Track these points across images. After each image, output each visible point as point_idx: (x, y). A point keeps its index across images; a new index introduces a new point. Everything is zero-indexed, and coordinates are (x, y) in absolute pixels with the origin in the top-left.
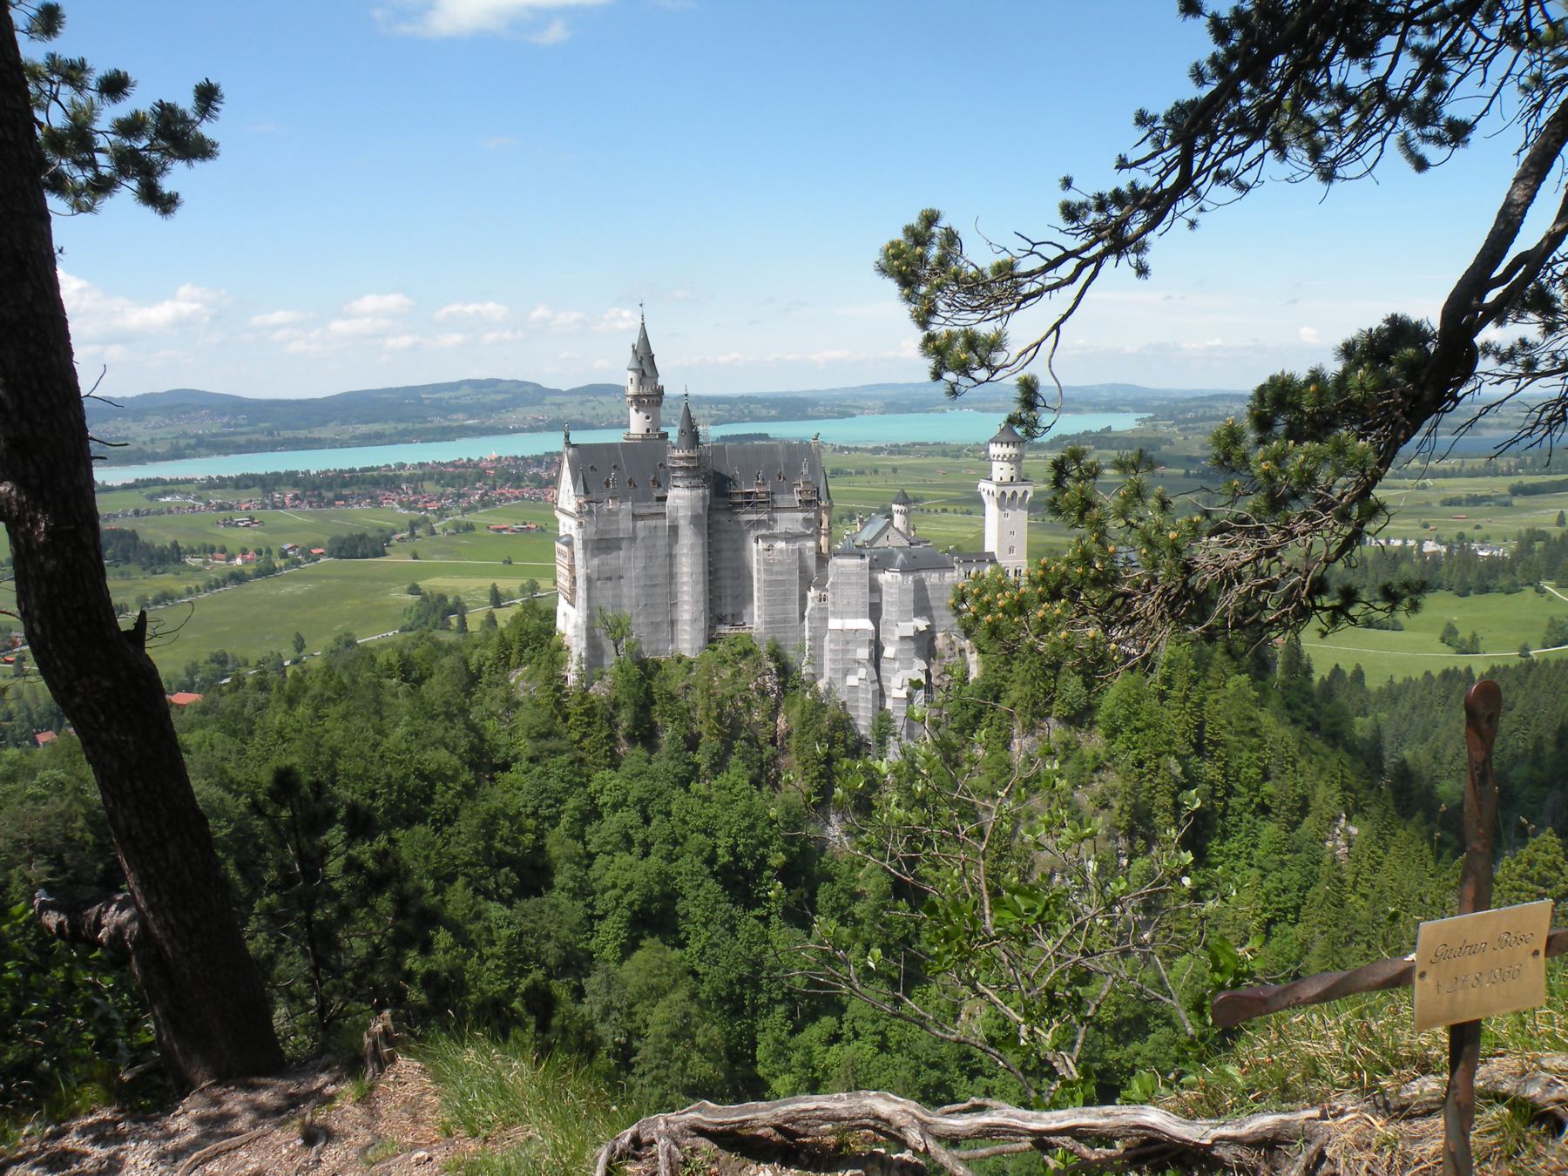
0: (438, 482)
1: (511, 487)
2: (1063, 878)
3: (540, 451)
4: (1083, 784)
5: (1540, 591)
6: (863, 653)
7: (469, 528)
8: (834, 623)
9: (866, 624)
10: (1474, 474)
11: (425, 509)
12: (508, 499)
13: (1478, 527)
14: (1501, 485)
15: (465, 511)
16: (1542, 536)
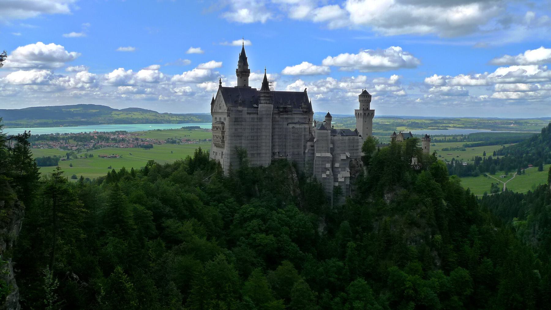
0: (75, 140)
1: (105, 142)
2: (411, 242)
3: (114, 130)
4: (413, 209)
5: (486, 176)
6: (328, 165)
7: (91, 156)
8: (318, 155)
9: (329, 155)
10: (449, 141)
11: (71, 149)
12: (105, 146)
13: (458, 157)
14: (460, 145)
15: (88, 150)
16: (480, 159)
